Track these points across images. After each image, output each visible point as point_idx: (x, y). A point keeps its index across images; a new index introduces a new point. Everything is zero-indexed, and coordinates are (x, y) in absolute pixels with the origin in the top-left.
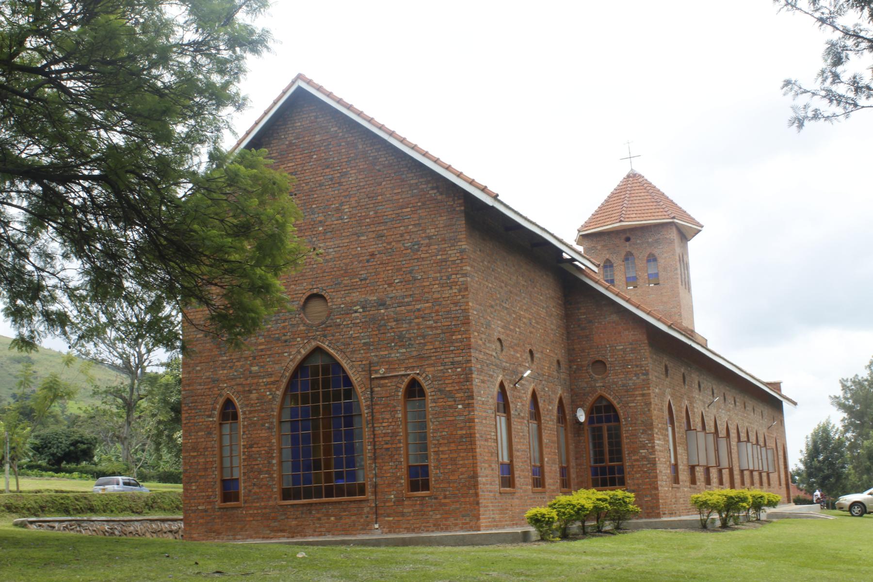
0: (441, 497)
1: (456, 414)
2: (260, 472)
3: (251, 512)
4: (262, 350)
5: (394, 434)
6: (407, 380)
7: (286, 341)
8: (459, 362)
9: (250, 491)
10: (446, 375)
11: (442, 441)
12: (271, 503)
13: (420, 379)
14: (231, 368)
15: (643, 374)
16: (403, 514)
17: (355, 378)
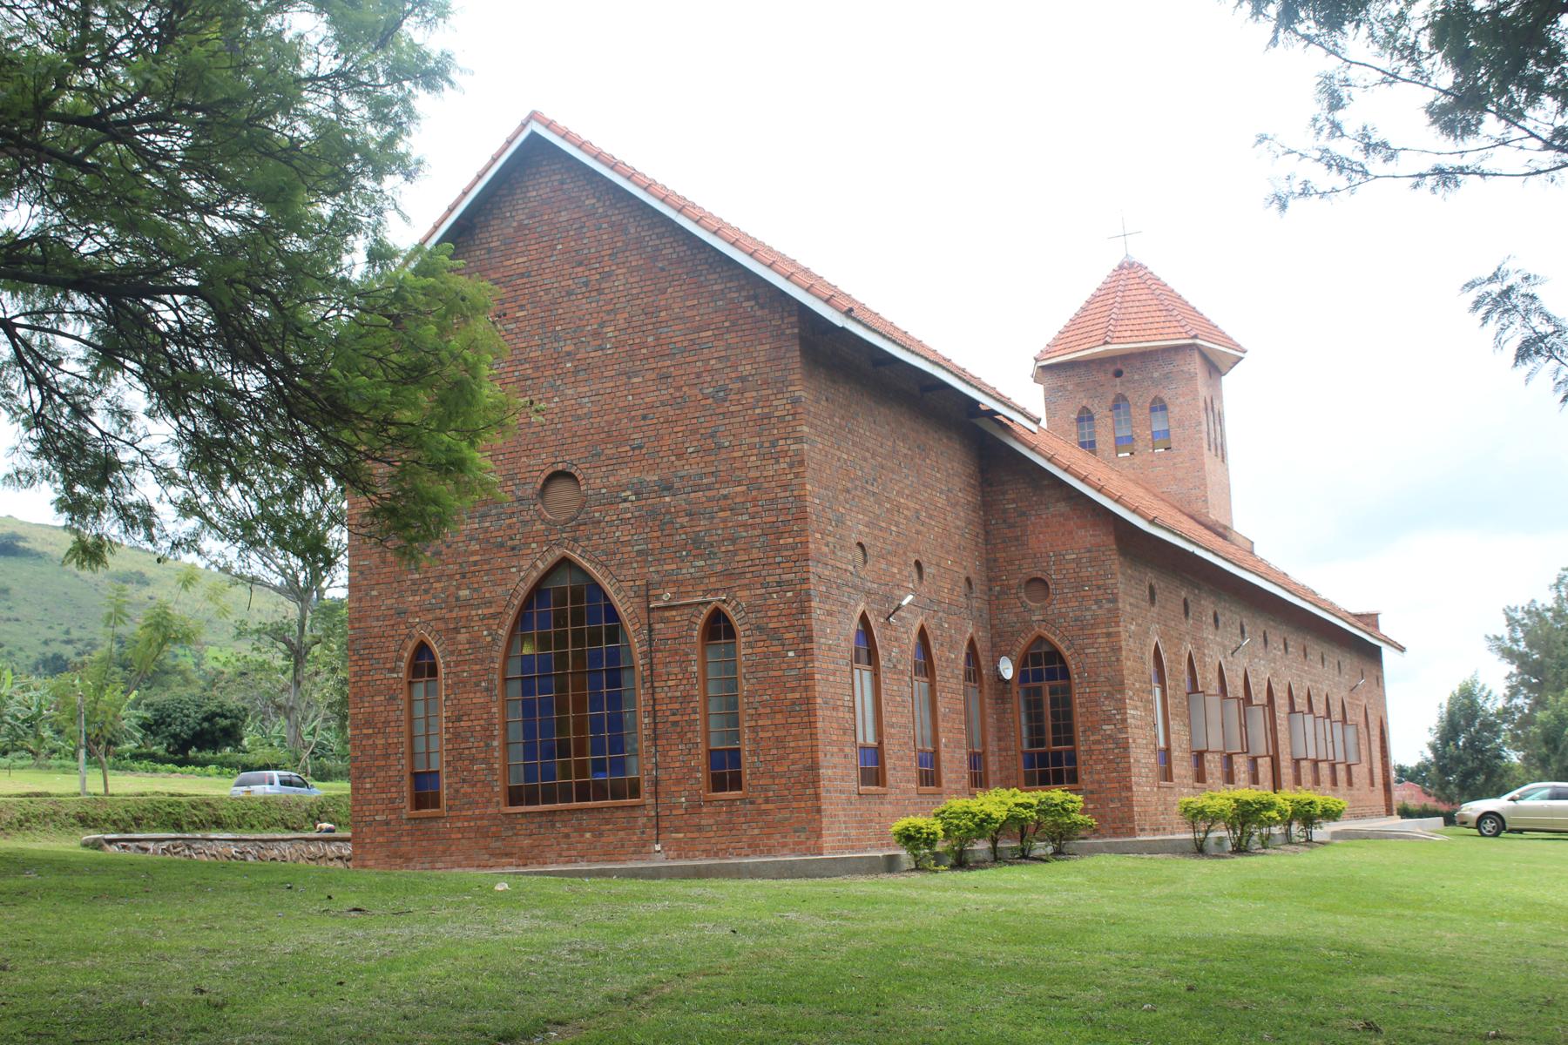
0: (760, 800)
1: (784, 666)
2: (473, 760)
3: (459, 824)
4: (476, 563)
5: (686, 699)
6: (706, 611)
7: (513, 549)
8: (790, 582)
9: (457, 791)
10: (770, 602)
11: (761, 710)
12: (490, 810)
13: (727, 609)
14: (426, 591)
15: (1109, 601)
16: (700, 828)
17: (624, 608)
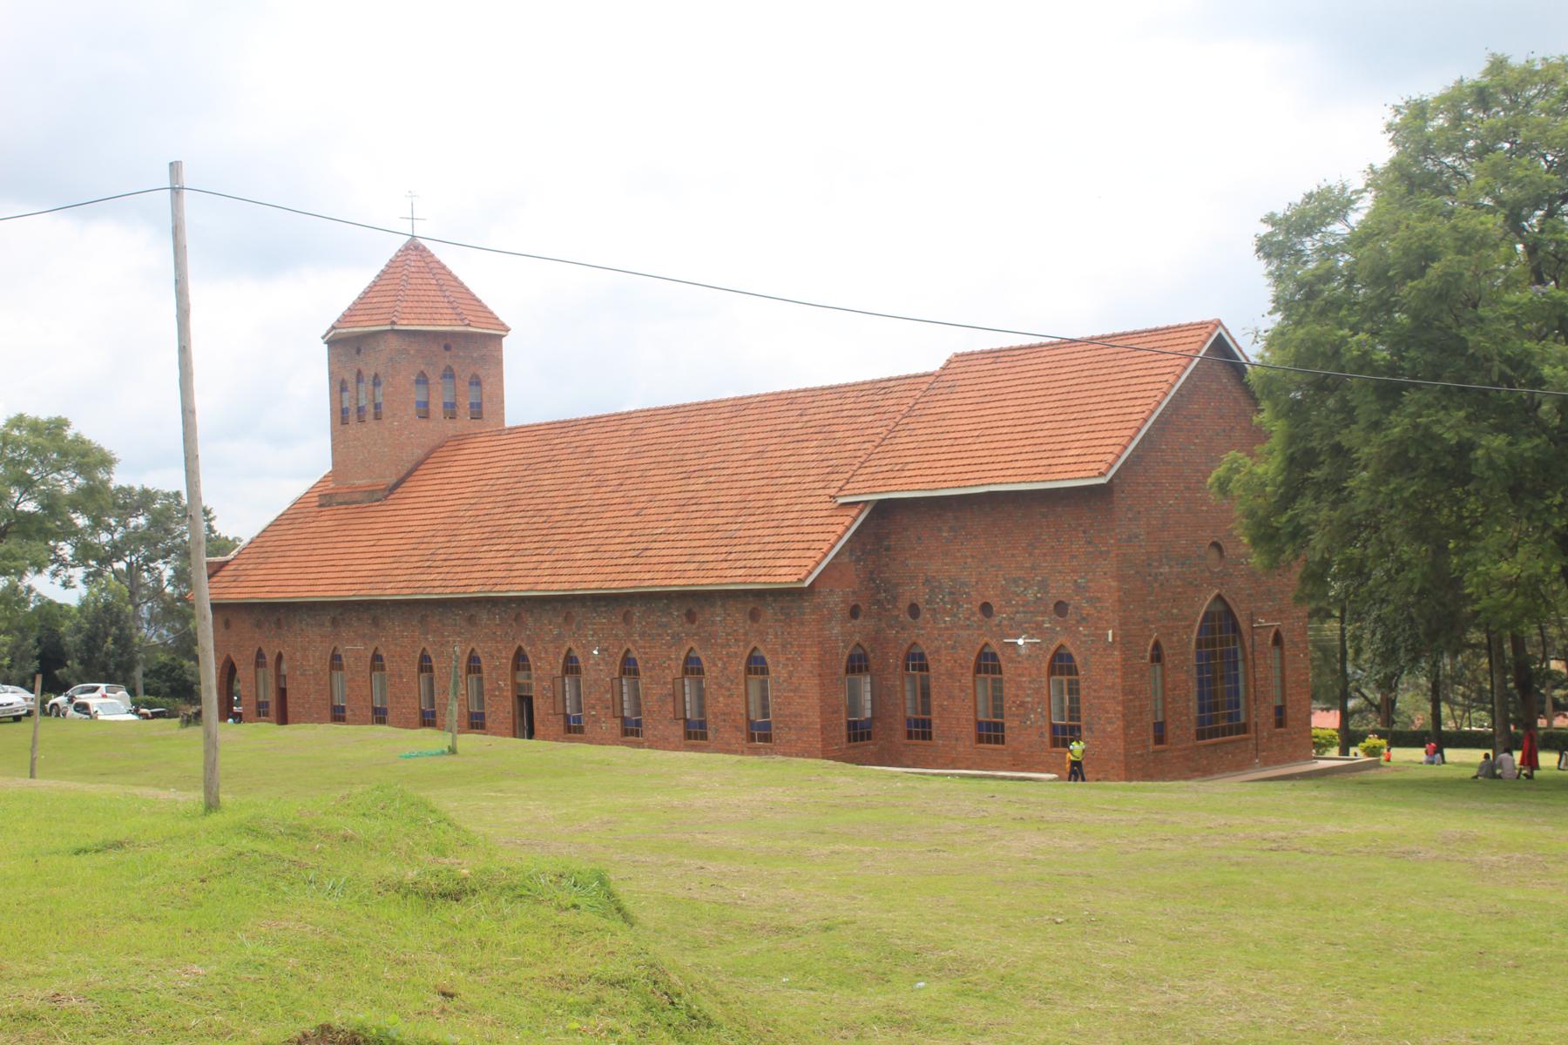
5: (1266, 678)
17: (1244, 625)
